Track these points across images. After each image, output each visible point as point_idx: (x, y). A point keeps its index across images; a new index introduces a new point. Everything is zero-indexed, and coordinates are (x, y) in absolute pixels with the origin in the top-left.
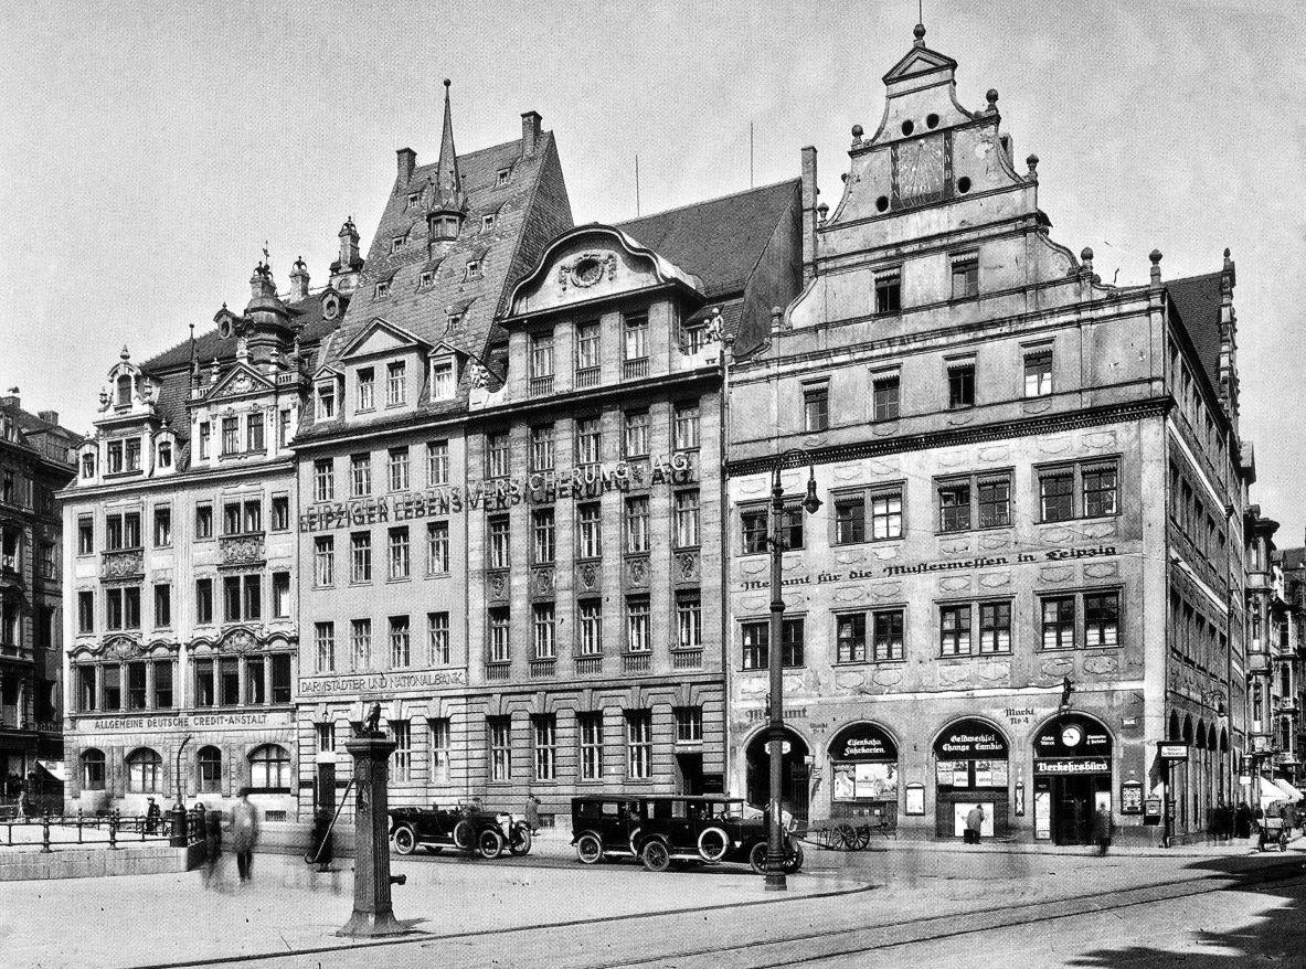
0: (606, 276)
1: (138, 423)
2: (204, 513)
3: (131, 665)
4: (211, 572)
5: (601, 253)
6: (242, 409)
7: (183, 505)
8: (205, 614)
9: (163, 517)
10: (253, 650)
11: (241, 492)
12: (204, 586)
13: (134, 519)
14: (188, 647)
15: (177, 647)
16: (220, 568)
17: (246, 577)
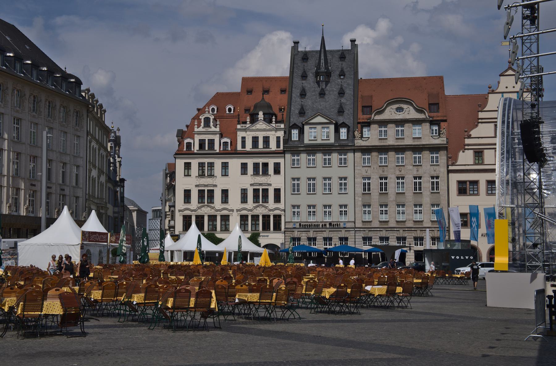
0: (406, 113)
1: (214, 133)
2: (244, 166)
3: (208, 216)
4: (247, 186)
5: (405, 106)
6: (261, 135)
7: (235, 164)
8: (244, 199)
9: (225, 166)
10: (266, 212)
11: (261, 161)
12: (244, 193)
13: (211, 165)
14: (237, 210)
15: (233, 211)
16: (251, 185)
17: (262, 189)
